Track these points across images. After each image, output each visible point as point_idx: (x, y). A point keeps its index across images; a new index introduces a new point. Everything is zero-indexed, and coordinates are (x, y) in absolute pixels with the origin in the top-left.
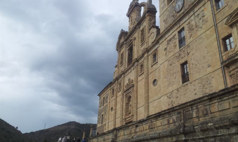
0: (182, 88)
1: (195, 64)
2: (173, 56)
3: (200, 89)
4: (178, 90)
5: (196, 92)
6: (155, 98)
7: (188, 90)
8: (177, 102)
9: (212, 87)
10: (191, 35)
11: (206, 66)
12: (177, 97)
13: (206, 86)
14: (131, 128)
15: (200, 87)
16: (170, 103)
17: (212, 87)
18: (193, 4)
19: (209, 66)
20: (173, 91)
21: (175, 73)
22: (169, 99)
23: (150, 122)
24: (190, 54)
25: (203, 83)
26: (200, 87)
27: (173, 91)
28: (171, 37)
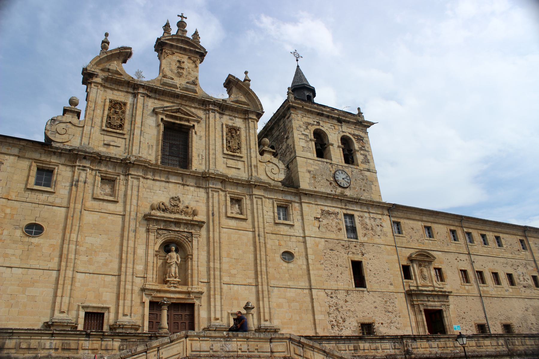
0: (354, 291)
1: (374, 273)
2: (337, 242)
3: (381, 303)
4: (347, 291)
5: (375, 305)
6: (290, 283)
7: (364, 298)
8: (346, 307)
9: (395, 307)
10: (365, 234)
11: (388, 282)
12: (346, 301)
13: (388, 304)
14: (444, 340)
15: (381, 301)
16: (333, 305)
17: (395, 307)
18: (373, 203)
19: (391, 284)
20: (338, 290)
21: (341, 266)
22: (329, 298)
23: (476, 339)
24: (365, 255)
25: (385, 299)
26: (381, 301)
27: (338, 290)
28: (331, 210)
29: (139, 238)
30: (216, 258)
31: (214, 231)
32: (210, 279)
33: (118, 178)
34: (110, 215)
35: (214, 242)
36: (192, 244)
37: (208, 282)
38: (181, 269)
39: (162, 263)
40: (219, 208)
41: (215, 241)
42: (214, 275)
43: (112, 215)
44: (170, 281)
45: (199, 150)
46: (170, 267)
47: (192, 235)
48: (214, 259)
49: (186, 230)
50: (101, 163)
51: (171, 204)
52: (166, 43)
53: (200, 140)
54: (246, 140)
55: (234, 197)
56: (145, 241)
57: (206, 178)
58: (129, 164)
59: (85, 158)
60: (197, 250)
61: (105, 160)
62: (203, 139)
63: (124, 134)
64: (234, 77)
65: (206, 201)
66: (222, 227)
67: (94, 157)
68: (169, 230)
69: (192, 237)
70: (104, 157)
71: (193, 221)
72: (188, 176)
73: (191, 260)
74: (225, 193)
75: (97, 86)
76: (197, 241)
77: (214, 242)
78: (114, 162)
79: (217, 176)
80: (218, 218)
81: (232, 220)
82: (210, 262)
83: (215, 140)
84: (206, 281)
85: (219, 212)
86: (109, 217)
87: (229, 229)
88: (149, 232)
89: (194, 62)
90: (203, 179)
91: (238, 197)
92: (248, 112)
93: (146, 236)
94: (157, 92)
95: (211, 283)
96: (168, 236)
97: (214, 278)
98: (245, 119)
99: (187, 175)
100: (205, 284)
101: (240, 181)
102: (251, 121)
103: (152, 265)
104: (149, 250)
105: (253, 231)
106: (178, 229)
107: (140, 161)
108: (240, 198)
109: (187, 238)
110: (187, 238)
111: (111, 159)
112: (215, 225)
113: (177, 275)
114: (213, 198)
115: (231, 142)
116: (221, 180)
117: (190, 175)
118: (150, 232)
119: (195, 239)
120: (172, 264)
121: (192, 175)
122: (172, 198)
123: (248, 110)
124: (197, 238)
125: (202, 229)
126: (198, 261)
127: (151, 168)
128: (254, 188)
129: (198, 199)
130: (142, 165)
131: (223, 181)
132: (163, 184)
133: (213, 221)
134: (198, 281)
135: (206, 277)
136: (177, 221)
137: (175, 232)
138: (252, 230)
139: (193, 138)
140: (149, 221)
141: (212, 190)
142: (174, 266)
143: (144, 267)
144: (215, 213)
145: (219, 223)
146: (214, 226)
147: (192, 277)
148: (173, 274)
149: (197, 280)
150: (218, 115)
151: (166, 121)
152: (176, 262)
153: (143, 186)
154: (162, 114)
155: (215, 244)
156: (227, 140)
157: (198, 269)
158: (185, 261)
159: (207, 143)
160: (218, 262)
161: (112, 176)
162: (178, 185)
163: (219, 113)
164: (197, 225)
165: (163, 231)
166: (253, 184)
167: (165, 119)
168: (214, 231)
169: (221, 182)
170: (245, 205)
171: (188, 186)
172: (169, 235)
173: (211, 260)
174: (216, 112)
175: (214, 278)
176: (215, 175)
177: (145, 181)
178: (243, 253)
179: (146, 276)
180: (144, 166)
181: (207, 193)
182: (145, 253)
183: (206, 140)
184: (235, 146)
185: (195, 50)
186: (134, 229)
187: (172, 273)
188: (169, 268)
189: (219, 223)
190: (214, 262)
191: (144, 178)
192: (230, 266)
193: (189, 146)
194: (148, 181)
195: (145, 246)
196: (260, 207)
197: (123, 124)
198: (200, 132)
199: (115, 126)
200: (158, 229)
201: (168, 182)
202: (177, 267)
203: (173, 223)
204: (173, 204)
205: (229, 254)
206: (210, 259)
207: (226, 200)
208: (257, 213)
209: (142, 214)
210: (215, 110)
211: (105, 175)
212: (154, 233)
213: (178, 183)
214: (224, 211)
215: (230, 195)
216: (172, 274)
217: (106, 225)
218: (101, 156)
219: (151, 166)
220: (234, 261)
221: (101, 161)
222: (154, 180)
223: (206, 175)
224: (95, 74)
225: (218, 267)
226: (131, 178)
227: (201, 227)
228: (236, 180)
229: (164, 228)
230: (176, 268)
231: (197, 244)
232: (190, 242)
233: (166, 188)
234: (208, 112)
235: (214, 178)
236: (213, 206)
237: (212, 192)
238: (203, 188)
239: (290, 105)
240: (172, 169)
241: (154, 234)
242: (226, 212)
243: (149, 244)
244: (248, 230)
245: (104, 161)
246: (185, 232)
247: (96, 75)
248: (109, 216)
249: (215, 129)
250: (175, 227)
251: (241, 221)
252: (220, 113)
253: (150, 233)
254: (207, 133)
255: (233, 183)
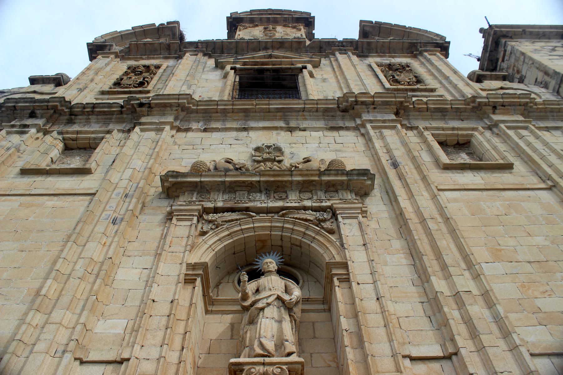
29: (133, 239)
30: (448, 260)
31: (411, 196)
32: (453, 340)
33: (108, 136)
34: (55, 198)
35: (423, 221)
36: (340, 238)
37: (448, 357)
38: (315, 337)
39: (232, 325)
40: (409, 151)
41: (426, 216)
42: (468, 321)
43: (61, 197)
44: (246, 368)
45: (324, 92)
46: (252, 322)
47: (334, 215)
48: (444, 267)
49: (308, 203)
50: (75, 123)
51: (255, 161)
52: (242, 18)
53: (324, 82)
54: (432, 74)
55: (446, 135)
56: (156, 244)
57: (351, 111)
58: (138, 109)
59: (32, 115)
60: (363, 248)
61: (83, 113)
62: (333, 81)
63: (148, 92)
64: (372, 22)
65: (363, 149)
66: (439, 190)
67: (55, 108)
68: (247, 209)
69: (337, 219)
70: (78, 108)
71: (329, 175)
72: (301, 113)
73: (345, 285)
74: (415, 132)
75: (108, 57)
76: (357, 226)
77: (423, 221)
78: (104, 113)
79: (377, 97)
80: (414, 171)
81: (463, 173)
82: (428, 280)
83: (359, 76)
84: (437, 351)
85: (414, 159)
86: (47, 203)
87: (466, 192)
88: (171, 219)
89: (294, 27)
90: (343, 116)
91: (458, 135)
92: (416, 47)
93: (161, 232)
94: (225, 51)
95: (463, 352)
96: (243, 227)
97: (474, 334)
98: (415, 57)
99: (297, 111)
100: (436, 366)
101: (447, 104)
102: (430, 55)
103: (165, 309)
104: (161, 265)
105: (549, 189)
106: (280, 204)
107: (167, 97)
108: (463, 135)
109: (319, 222)
110: (319, 222)
111: (96, 108)
112: (408, 181)
113: (291, 347)
114: (382, 137)
115: (398, 75)
116: (394, 107)
117: (304, 110)
118: (174, 218)
119: (347, 221)
120: (260, 305)
121: (310, 110)
122: (257, 149)
123: (414, 43)
124: (356, 218)
125: (368, 200)
126: (374, 282)
127: (197, 111)
128: (494, 113)
129: (338, 147)
130: (171, 105)
131: (402, 112)
132: (234, 134)
133: (401, 177)
134: (394, 356)
135: (430, 334)
136: (272, 179)
137: (270, 215)
138: (543, 186)
139: (309, 87)
140: (176, 199)
141: (374, 128)
142: (272, 312)
143: (131, 323)
144: (399, 160)
145: (424, 178)
146: (406, 186)
147: (360, 343)
148: (270, 345)
149: (388, 352)
150: (355, 58)
151: (241, 70)
152: (279, 298)
153: (175, 143)
154: (234, 63)
155: (431, 224)
156: (385, 76)
157: (382, 307)
158: (329, 310)
159: (341, 81)
160: (467, 274)
161: (93, 136)
162: (275, 132)
163: (357, 57)
164: (346, 186)
165: (225, 213)
166: (486, 104)
167: (238, 66)
168: (411, 196)
169: (397, 114)
170: (486, 144)
171: (304, 130)
172: (247, 223)
173: (429, 270)
174: (350, 53)
175: (474, 334)
176: (373, 97)
177: (182, 135)
178: (553, 243)
179: (125, 355)
180: (179, 105)
181: (363, 135)
182: (145, 279)
183: (338, 82)
184: (410, 79)
185: (293, 18)
186: (122, 217)
187: (263, 341)
188: (252, 327)
189: (424, 178)
190: (448, 277)
191: (179, 130)
192: (523, 286)
193: (300, 90)
194: (190, 134)
195: (152, 258)
196: (531, 139)
197: (147, 82)
198: (322, 75)
199: (130, 85)
200: (207, 211)
201: (245, 129)
202: (287, 318)
203: (260, 192)
204: (260, 159)
205: (501, 250)
206: (425, 271)
207: (425, 141)
208: (535, 150)
209: (157, 187)
210: (345, 50)
211: (75, 136)
212: (191, 220)
213: (276, 128)
214: (425, 157)
215: (433, 132)
216: (262, 345)
217: (30, 219)
218: (71, 108)
219: (198, 105)
220: (529, 268)
221: (73, 117)
222: (205, 130)
223: (347, 101)
224: (106, 46)
225: (475, 291)
226: (142, 130)
227: (364, 194)
228: (434, 104)
229: (228, 205)
230: (280, 322)
231: (358, 233)
232: (331, 232)
233: (239, 138)
234: (330, 56)
235: (373, 103)
236: (389, 151)
237: (377, 131)
238: (347, 129)
239: (495, 31)
240: (252, 105)
241: (188, 223)
242: (436, 161)
243: (166, 247)
244: (528, 186)
245: (80, 117)
246: (305, 208)
247: (108, 47)
248: (52, 200)
249: (354, 66)
250: (268, 197)
251: (493, 173)
252: (358, 56)
253: (174, 220)
254: (338, 73)
255: (429, 113)
